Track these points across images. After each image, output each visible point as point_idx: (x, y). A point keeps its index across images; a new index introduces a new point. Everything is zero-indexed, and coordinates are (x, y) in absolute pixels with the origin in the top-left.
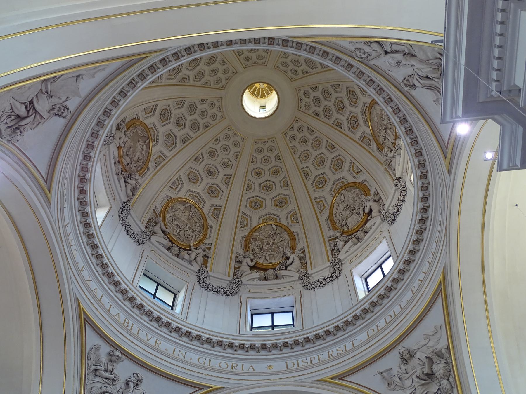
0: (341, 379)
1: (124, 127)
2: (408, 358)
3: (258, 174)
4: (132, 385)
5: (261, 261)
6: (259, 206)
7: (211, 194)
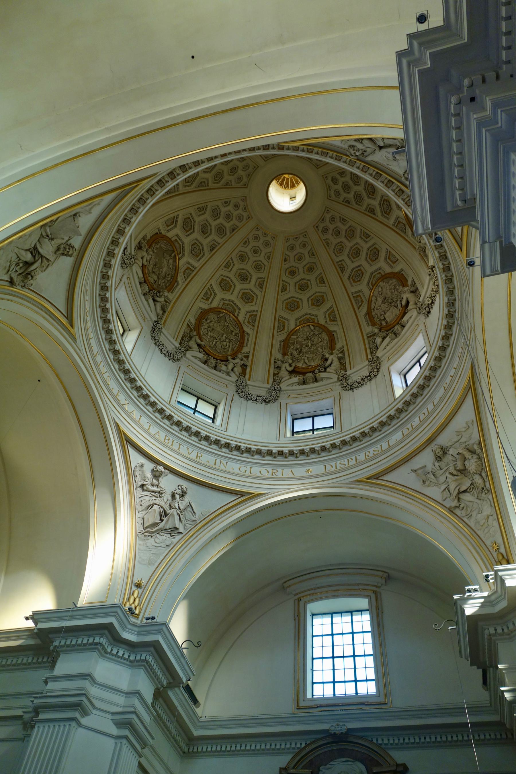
0: (377, 479)
1: (145, 246)
2: (441, 455)
3: (292, 273)
4: (177, 496)
5: (300, 365)
6: (296, 307)
7: (245, 300)
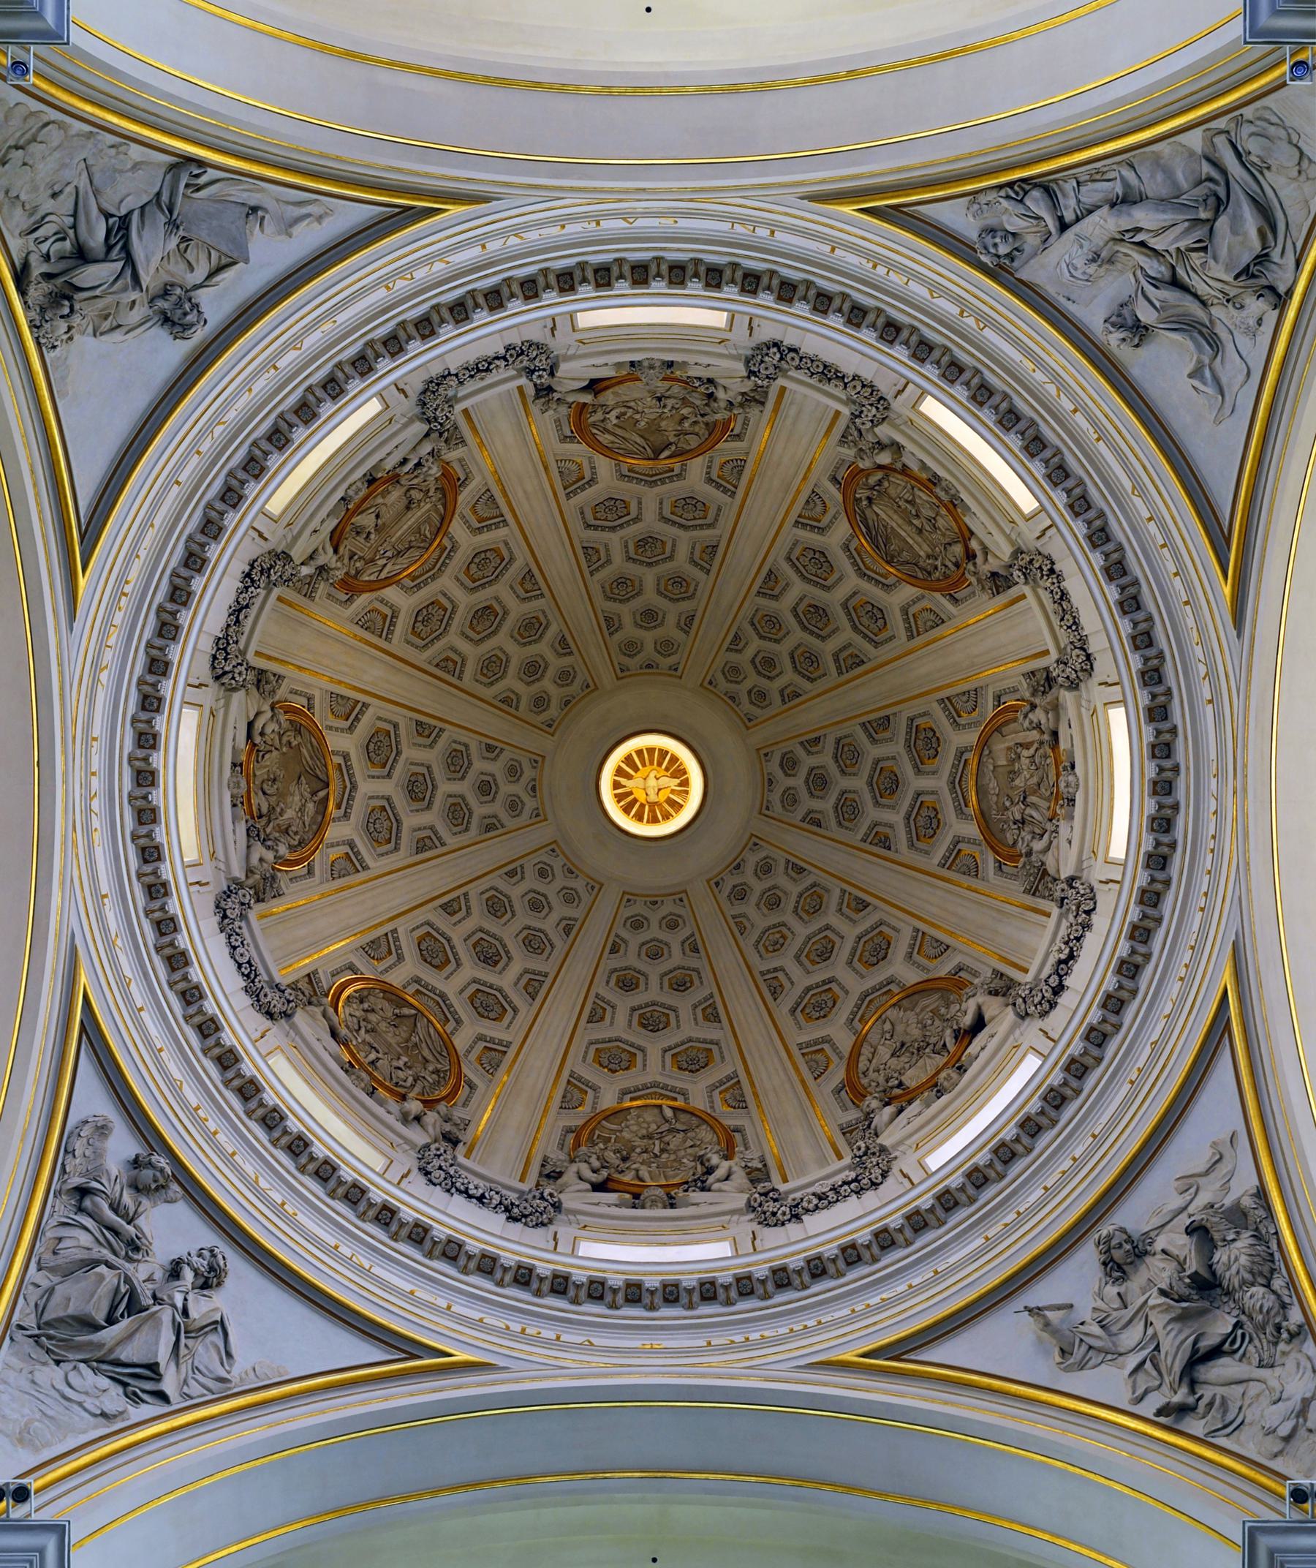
6: (624, 1064)
7: (480, 1010)
